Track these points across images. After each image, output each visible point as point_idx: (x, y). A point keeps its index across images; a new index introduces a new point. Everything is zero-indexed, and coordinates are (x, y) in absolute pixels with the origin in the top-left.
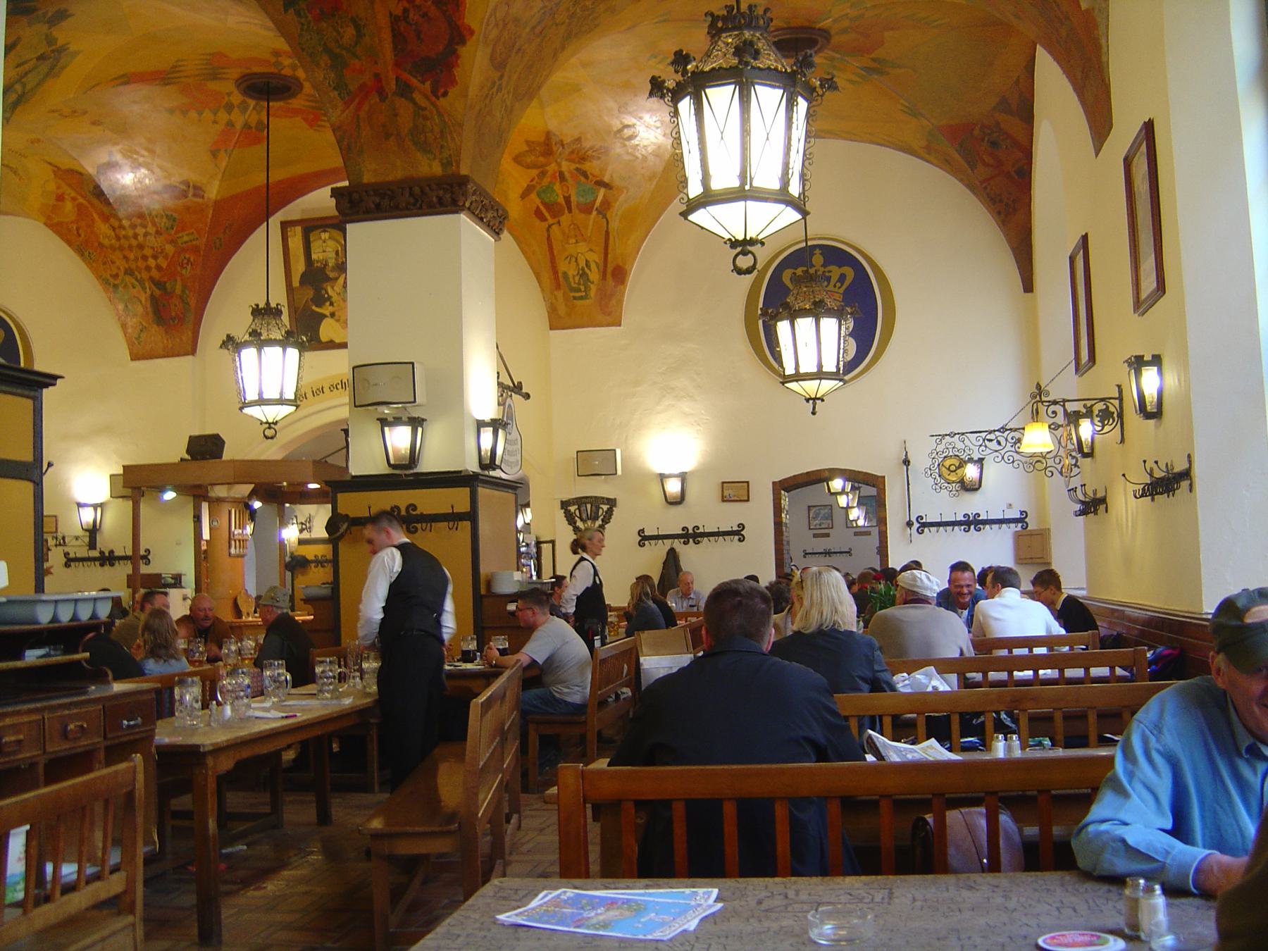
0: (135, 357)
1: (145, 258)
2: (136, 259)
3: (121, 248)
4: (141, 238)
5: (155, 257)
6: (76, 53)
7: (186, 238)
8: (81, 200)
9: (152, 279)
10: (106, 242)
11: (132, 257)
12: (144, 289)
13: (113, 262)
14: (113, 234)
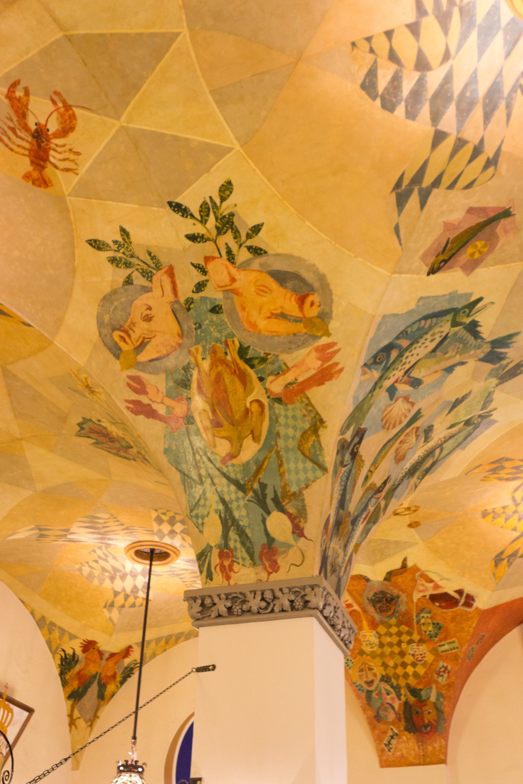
0: (385, 764)
1: (404, 665)
2: (395, 667)
3: (382, 655)
4: (404, 646)
5: (414, 665)
6: (495, 422)
7: (446, 647)
8: (356, 607)
9: (408, 686)
10: (367, 649)
11: (391, 664)
12: (399, 696)
13: (371, 669)
14: (376, 641)
